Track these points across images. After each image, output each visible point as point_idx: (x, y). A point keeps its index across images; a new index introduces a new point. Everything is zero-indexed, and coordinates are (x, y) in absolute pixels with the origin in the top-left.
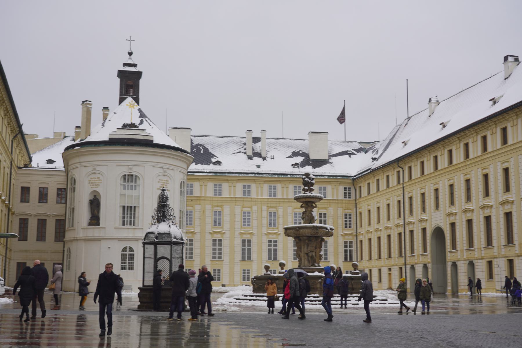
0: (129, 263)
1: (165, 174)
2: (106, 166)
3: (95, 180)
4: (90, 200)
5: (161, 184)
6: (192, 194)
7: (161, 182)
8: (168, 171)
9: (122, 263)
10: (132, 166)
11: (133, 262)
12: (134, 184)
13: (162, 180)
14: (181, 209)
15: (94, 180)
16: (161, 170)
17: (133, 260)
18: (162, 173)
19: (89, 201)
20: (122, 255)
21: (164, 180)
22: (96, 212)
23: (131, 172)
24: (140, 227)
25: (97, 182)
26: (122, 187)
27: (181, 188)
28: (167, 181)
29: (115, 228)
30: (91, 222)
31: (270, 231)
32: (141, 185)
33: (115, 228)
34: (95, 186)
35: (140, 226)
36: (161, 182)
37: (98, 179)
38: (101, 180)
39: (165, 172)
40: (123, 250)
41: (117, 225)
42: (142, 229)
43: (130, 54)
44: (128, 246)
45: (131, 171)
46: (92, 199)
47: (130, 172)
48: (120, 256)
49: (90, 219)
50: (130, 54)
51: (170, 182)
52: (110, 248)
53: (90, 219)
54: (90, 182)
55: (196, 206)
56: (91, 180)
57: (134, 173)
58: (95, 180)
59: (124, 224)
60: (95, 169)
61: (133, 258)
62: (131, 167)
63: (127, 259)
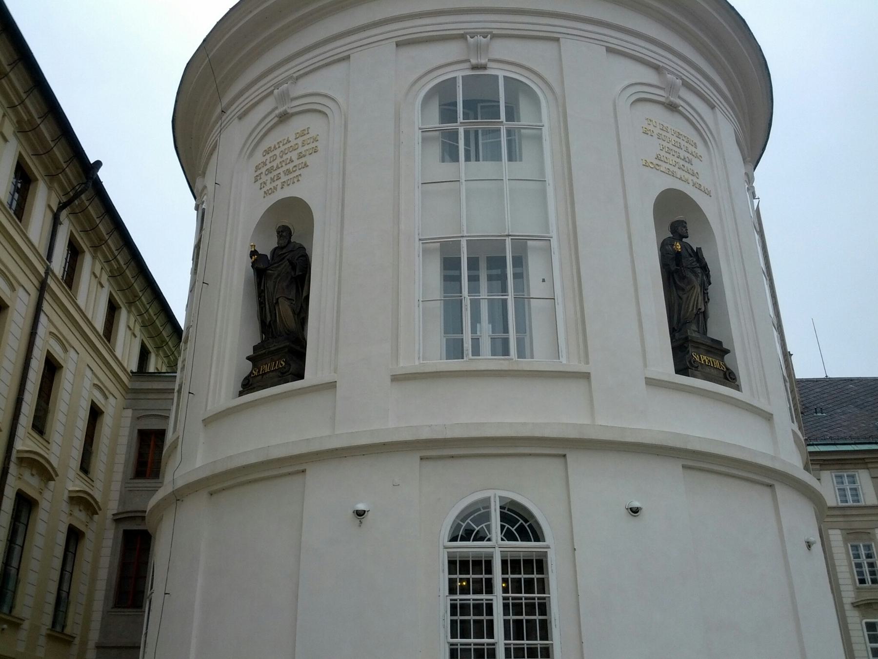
0: (516, 630)
2: (343, 66)
3: (283, 153)
4: (253, 253)
9: (459, 629)
11: (544, 625)
15: (277, 152)
16: (650, 76)
17: (543, 608)
18: (661, 95)
19: (250, 261)
20: (457, 565)
22: (285, 309)
23: (484, 67)
24: (568, 362)
25: (294, 155)
26: (436, 150)
29: (396, 379)
30: (255, 373)
31: (867, 596)
32: (545, 132)
33: (396, 379)
34: (284, 178)
35: (564, 360)
37: (299, 141)
38: (316, 140)
40: (456, 527)
42: (586, 376)
45: (483, 61)
46: (267, 248)
47: (475, 67)
48: (443, 578)
49: (249, 358)
52: (368, 517)
53: (249, 358)
54: (263, 170)
56: (268, 157)
58: (283, 153)
59: (455, 350)
60: (284, 97)
61: (543, 586)
63: (497, 599)
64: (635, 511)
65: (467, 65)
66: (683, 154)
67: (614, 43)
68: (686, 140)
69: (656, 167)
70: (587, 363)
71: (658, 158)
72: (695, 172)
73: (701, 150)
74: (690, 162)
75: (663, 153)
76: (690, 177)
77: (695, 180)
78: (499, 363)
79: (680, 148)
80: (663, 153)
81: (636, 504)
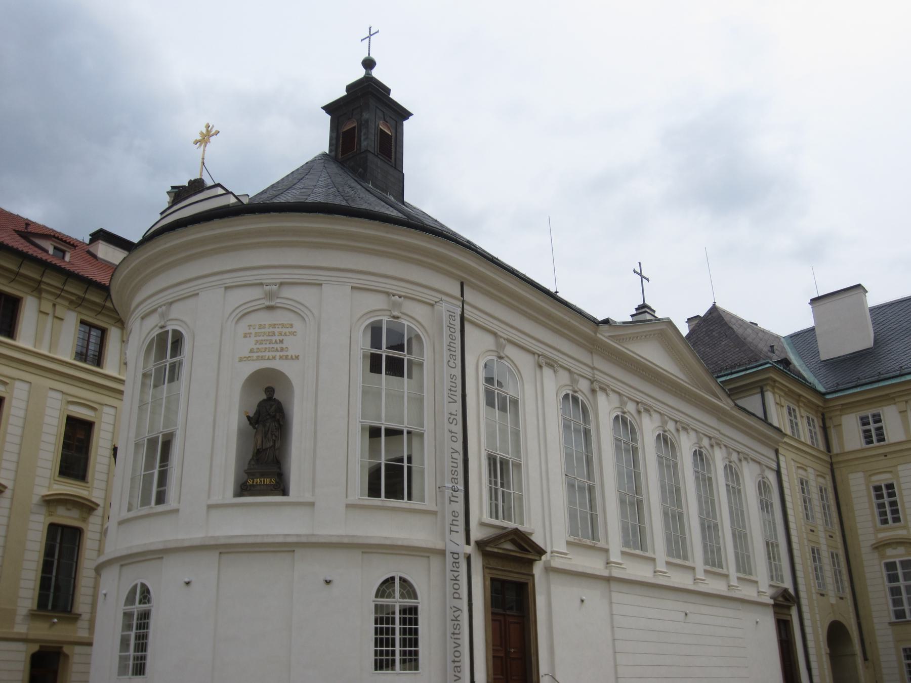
1: (273, 303)
5: (257, 341)
6: (884, 440)
7: (256, 335)
8: (287, 292)
10: (164, 305)
12: (169, 360)
13: (261, 327)
14: (375, 423)
21: (274, 326)
27: (376, 343)
28: (283, 326)
36: (256, 335)
39: (270, 295)
41: (125, 515)
43: (369, 64)
44: (139, 582)
47: (162, 327)
50: (369, 64)
51: (298, 325)
55: (900, 468)
57: (170, 328)
62: (164, 308)
64: (188, 583)
65: (157, 328)
66: (274, 338)
67: (229, 282)
68: (280, 326)
69: (248, 358)
70: (179, 503)
71: (252, 351)
72: (284, 347)
73: (298, 325)
74: (281, 342)
75: (255, 347)
76: (278, 354)
77: (282, 354)
78: (145, 510)
79: (274, 334)
80: (258, 346)
81: (187, 580)
